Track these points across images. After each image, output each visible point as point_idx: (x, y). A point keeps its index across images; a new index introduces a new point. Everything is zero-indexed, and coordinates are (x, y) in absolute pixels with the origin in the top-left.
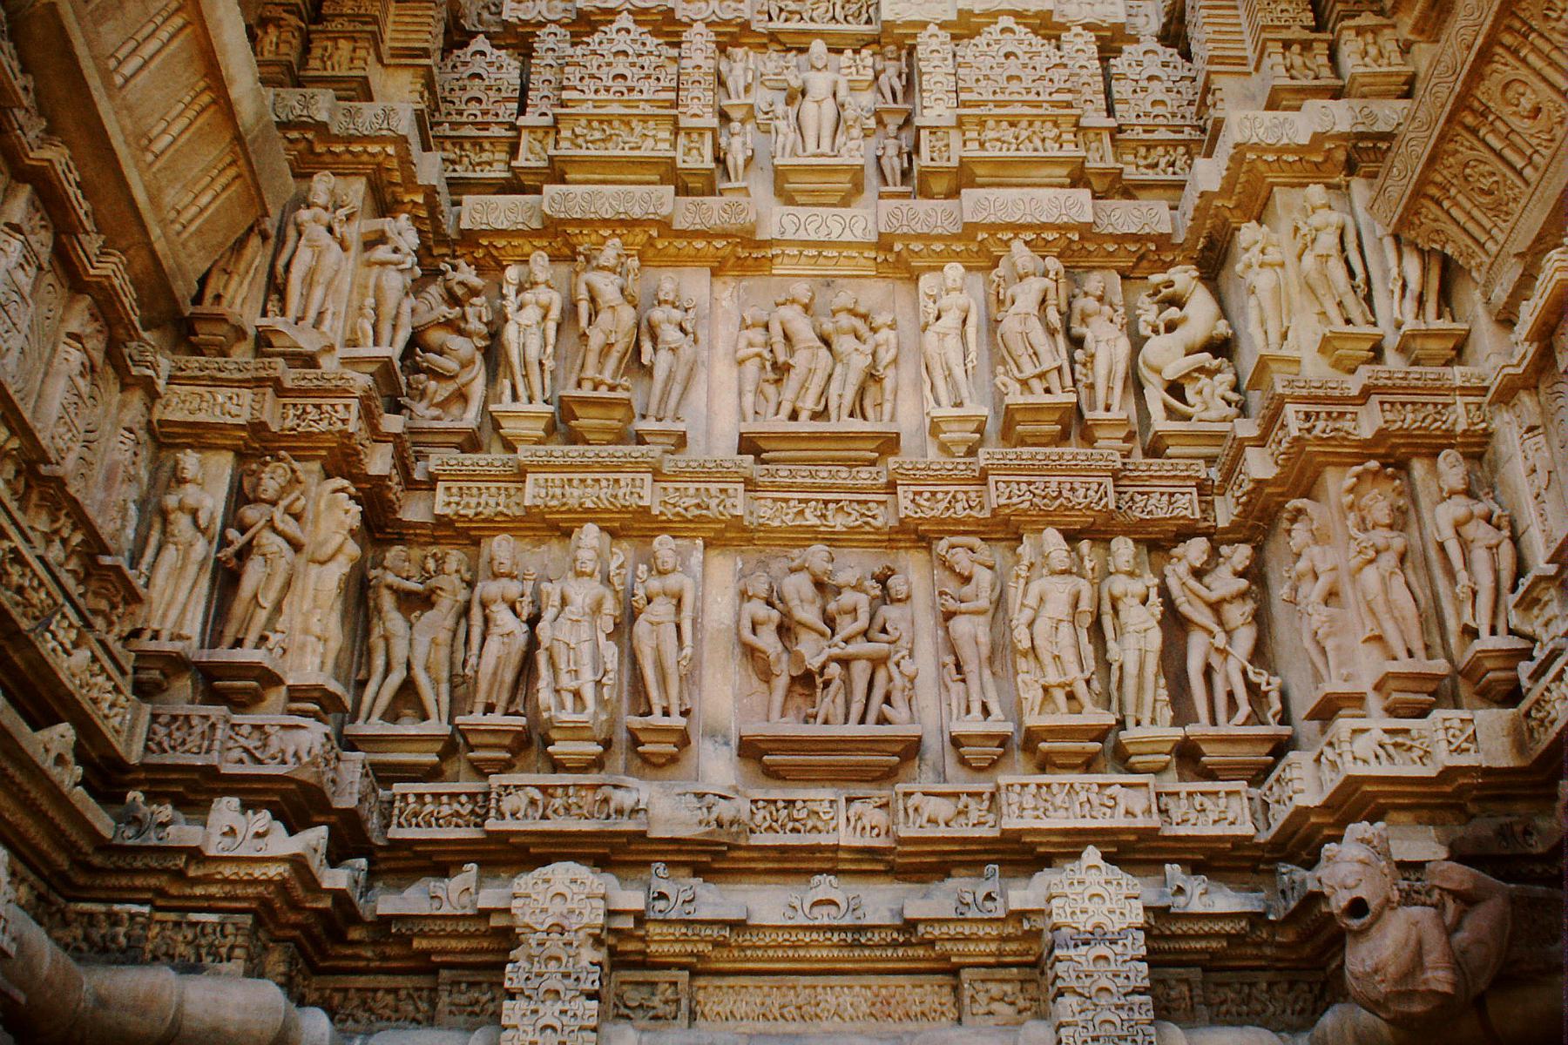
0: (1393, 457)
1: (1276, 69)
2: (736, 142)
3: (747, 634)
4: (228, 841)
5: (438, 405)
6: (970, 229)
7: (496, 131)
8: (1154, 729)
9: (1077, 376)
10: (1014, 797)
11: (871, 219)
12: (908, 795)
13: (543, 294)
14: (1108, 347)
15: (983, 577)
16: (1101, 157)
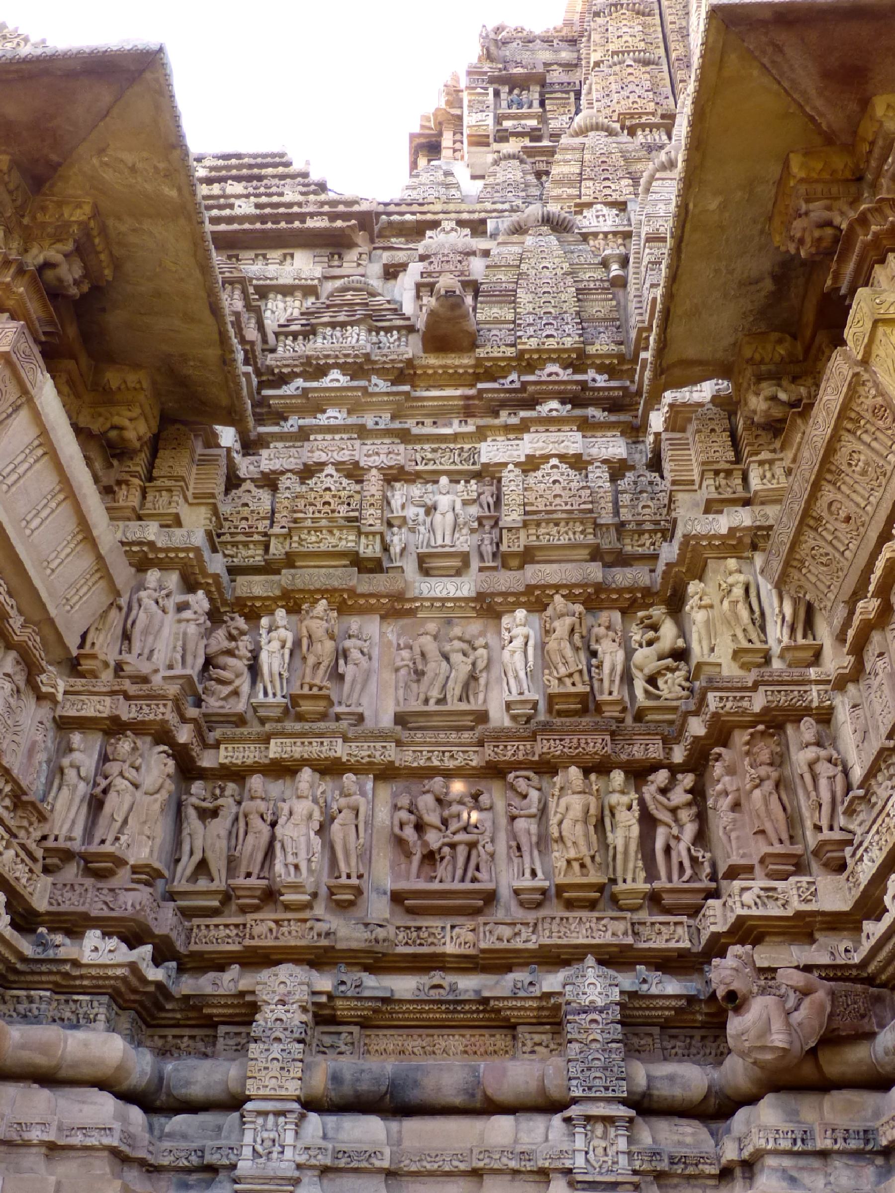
0: (775, 722)
1: (708, 490)
2: (396, 539)
3: (397, 830)
4: (94, 955)
5: (222, 699)
6: (530, 589)
7: (256, 537)
8: (633, 882)
9: (593, 674)
10: (546, 926)
11: (473, 584)
12: (485, 924)
13: (282, 632)
14: (611, 656)
15: (534, 795)
16: (608, 542)
